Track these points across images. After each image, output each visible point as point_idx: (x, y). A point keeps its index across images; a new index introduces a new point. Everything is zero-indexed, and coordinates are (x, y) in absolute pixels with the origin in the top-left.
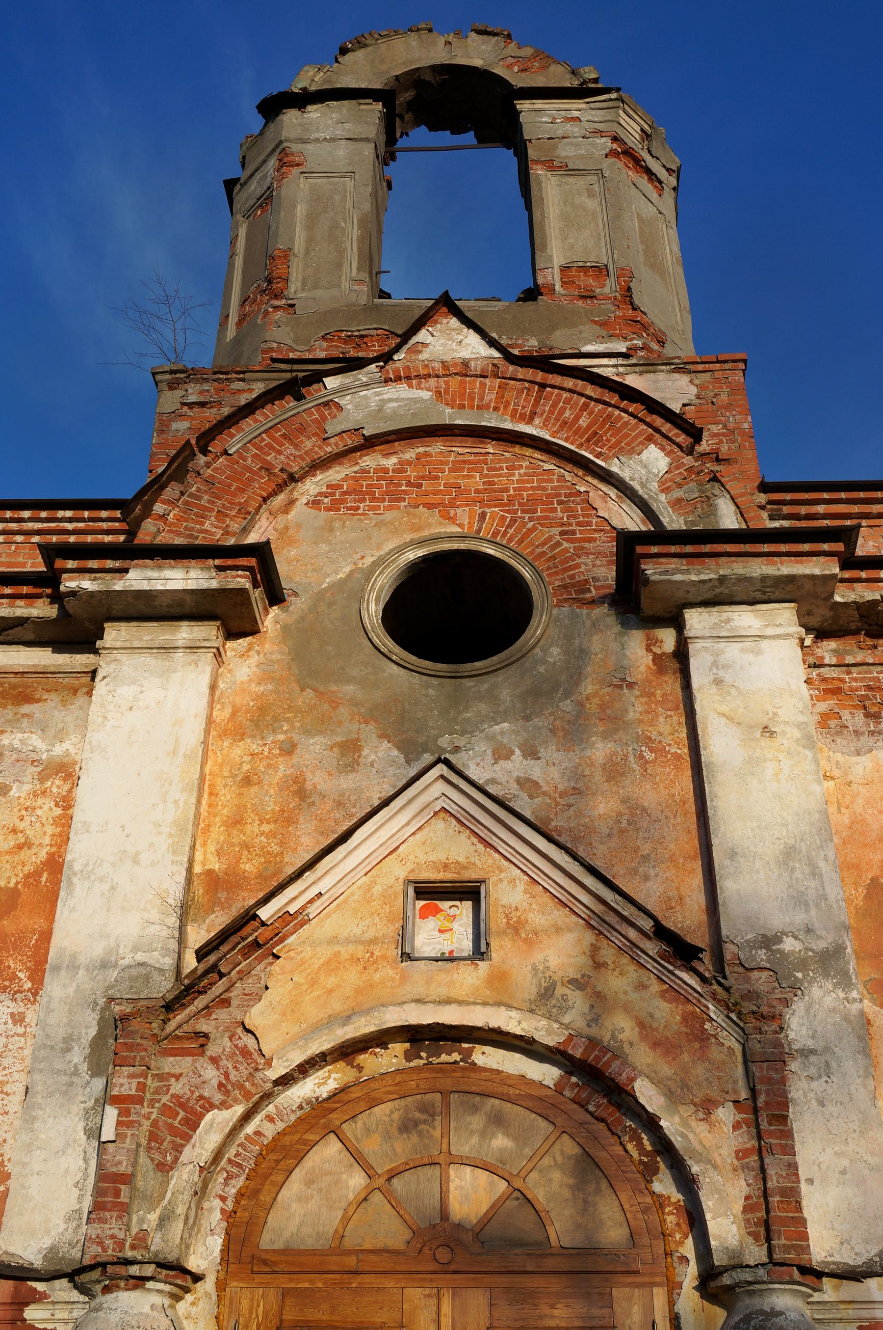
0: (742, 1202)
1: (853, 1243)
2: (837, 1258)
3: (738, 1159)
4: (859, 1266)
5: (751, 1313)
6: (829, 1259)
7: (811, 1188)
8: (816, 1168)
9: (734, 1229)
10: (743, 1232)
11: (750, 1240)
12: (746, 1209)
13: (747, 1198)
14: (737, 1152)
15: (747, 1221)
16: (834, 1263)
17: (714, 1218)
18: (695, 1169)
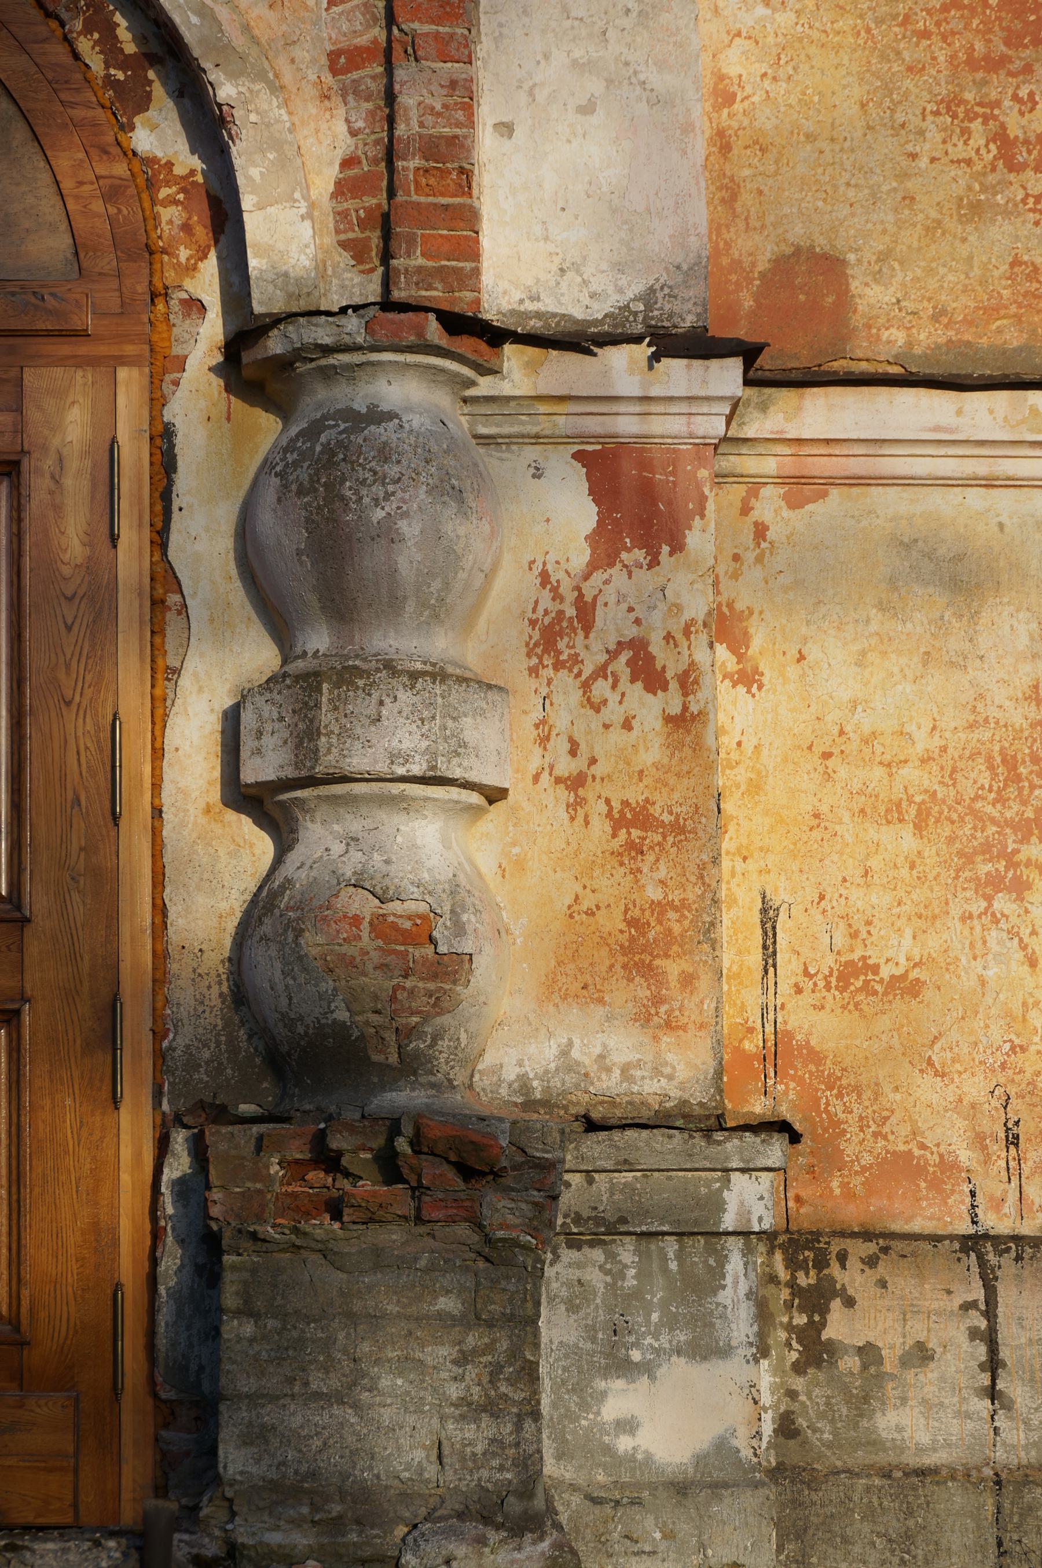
0: (333, 172)
1: (588, 271)
2: (548, 304)
3: (334, 71)
4: (596, 322)
5: (325, 417)
6: (530, 306)
7: (507, 145)
8: (523, 98)
9: (306, 230)
10: (329, 240)
11: (345, 258)
12: (341, 189)
13: (347, 163)
14: (333, 57)
15: (342, 216)
16: (538, 315)
17: (260, 207)
18: (226, 91)
